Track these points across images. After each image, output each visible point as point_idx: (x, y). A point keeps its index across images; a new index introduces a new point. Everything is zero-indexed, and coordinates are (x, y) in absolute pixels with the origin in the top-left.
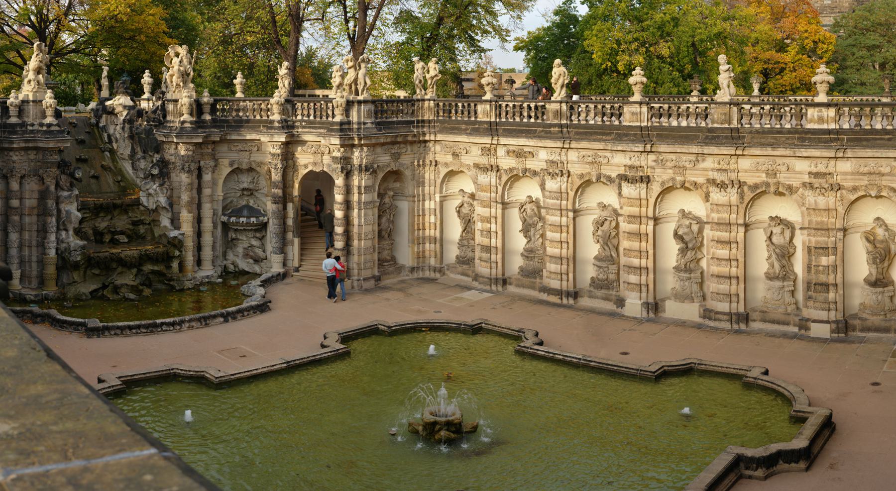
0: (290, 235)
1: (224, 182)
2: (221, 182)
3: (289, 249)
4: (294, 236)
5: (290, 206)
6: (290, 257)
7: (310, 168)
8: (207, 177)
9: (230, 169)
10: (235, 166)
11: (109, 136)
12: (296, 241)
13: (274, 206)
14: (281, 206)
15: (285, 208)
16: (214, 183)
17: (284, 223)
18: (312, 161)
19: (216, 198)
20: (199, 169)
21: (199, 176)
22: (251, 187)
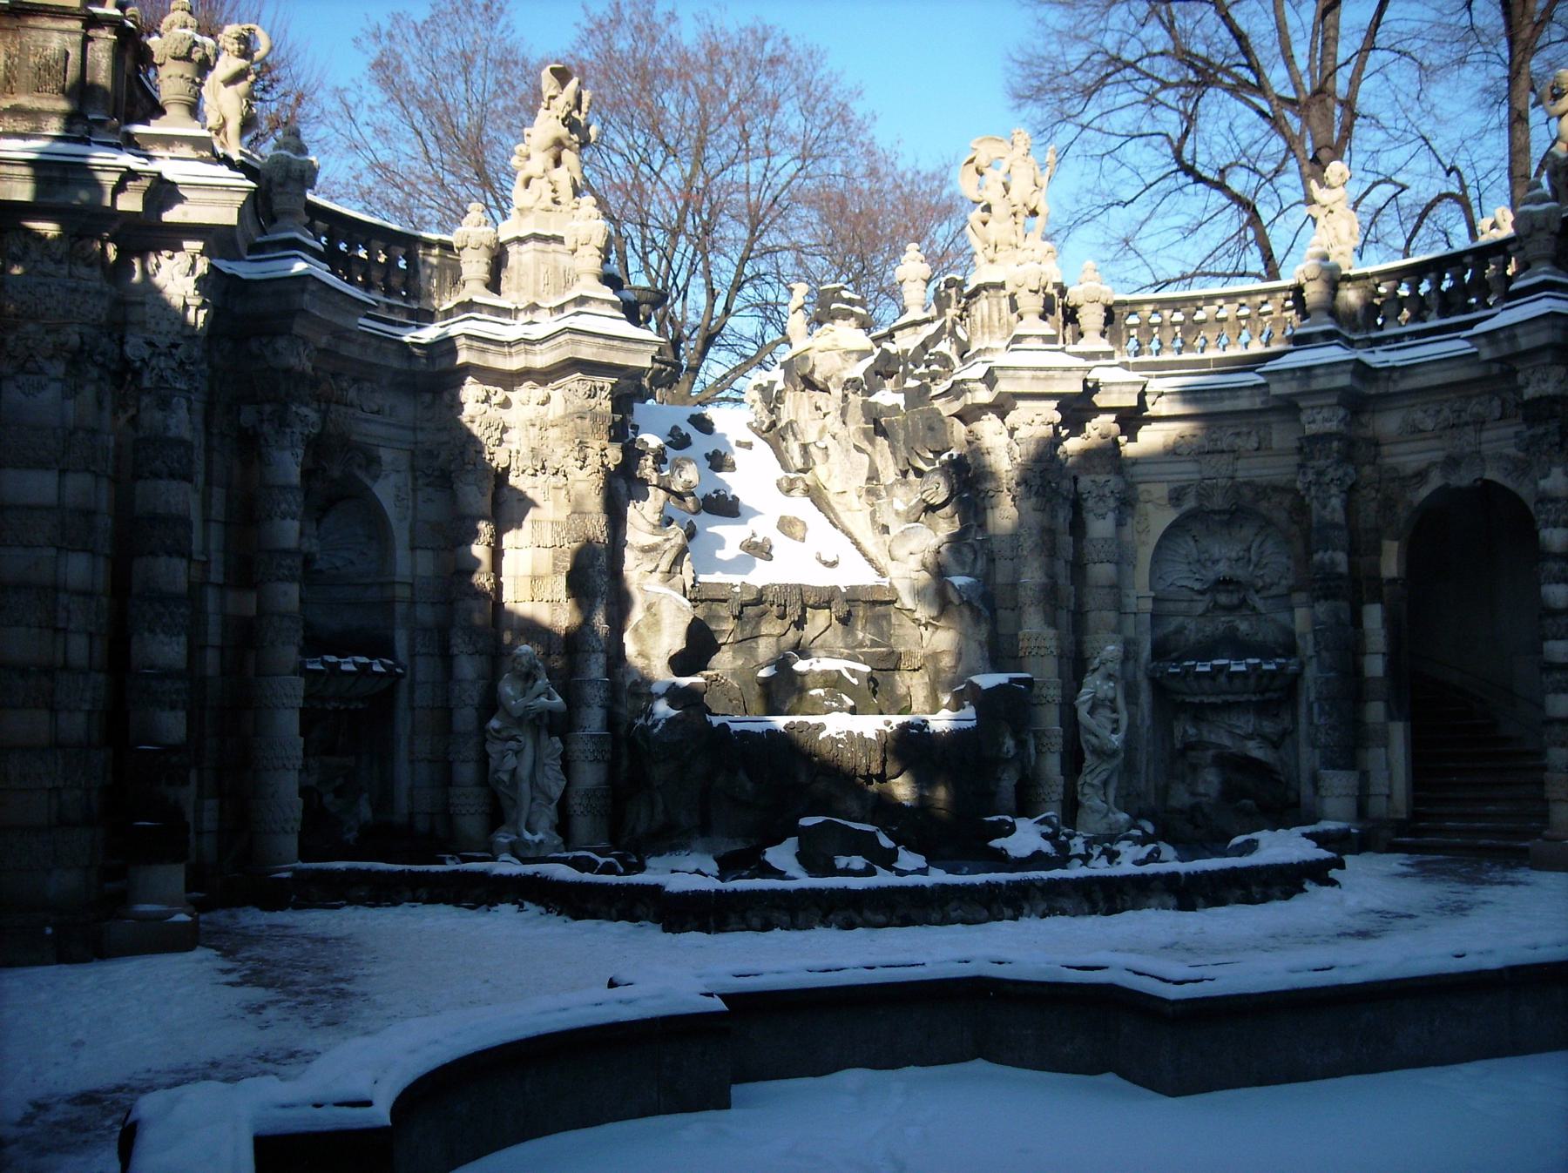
0: (1375, 711)
1: (1156, 559)
2: (1145, 555)
3: (1374, 758)
4: (1391, 717)
5: (1373, 616)
6: (1378, 785)
7: (1436, 481)
8: (1100, 527)
9: (1169, 516)
10: (1190, 503)
11: (805, 448)
12: (1398, 732)
13: (1322, 608)
14: (1344, 605)
15: (1357, 619)
16: (1122, 558)
17: (1358, 670)
18: (1439, 456)
19: (1131, 603)
20: (1077, 505)
21: (1078, 527)
22: (1241, 573)
